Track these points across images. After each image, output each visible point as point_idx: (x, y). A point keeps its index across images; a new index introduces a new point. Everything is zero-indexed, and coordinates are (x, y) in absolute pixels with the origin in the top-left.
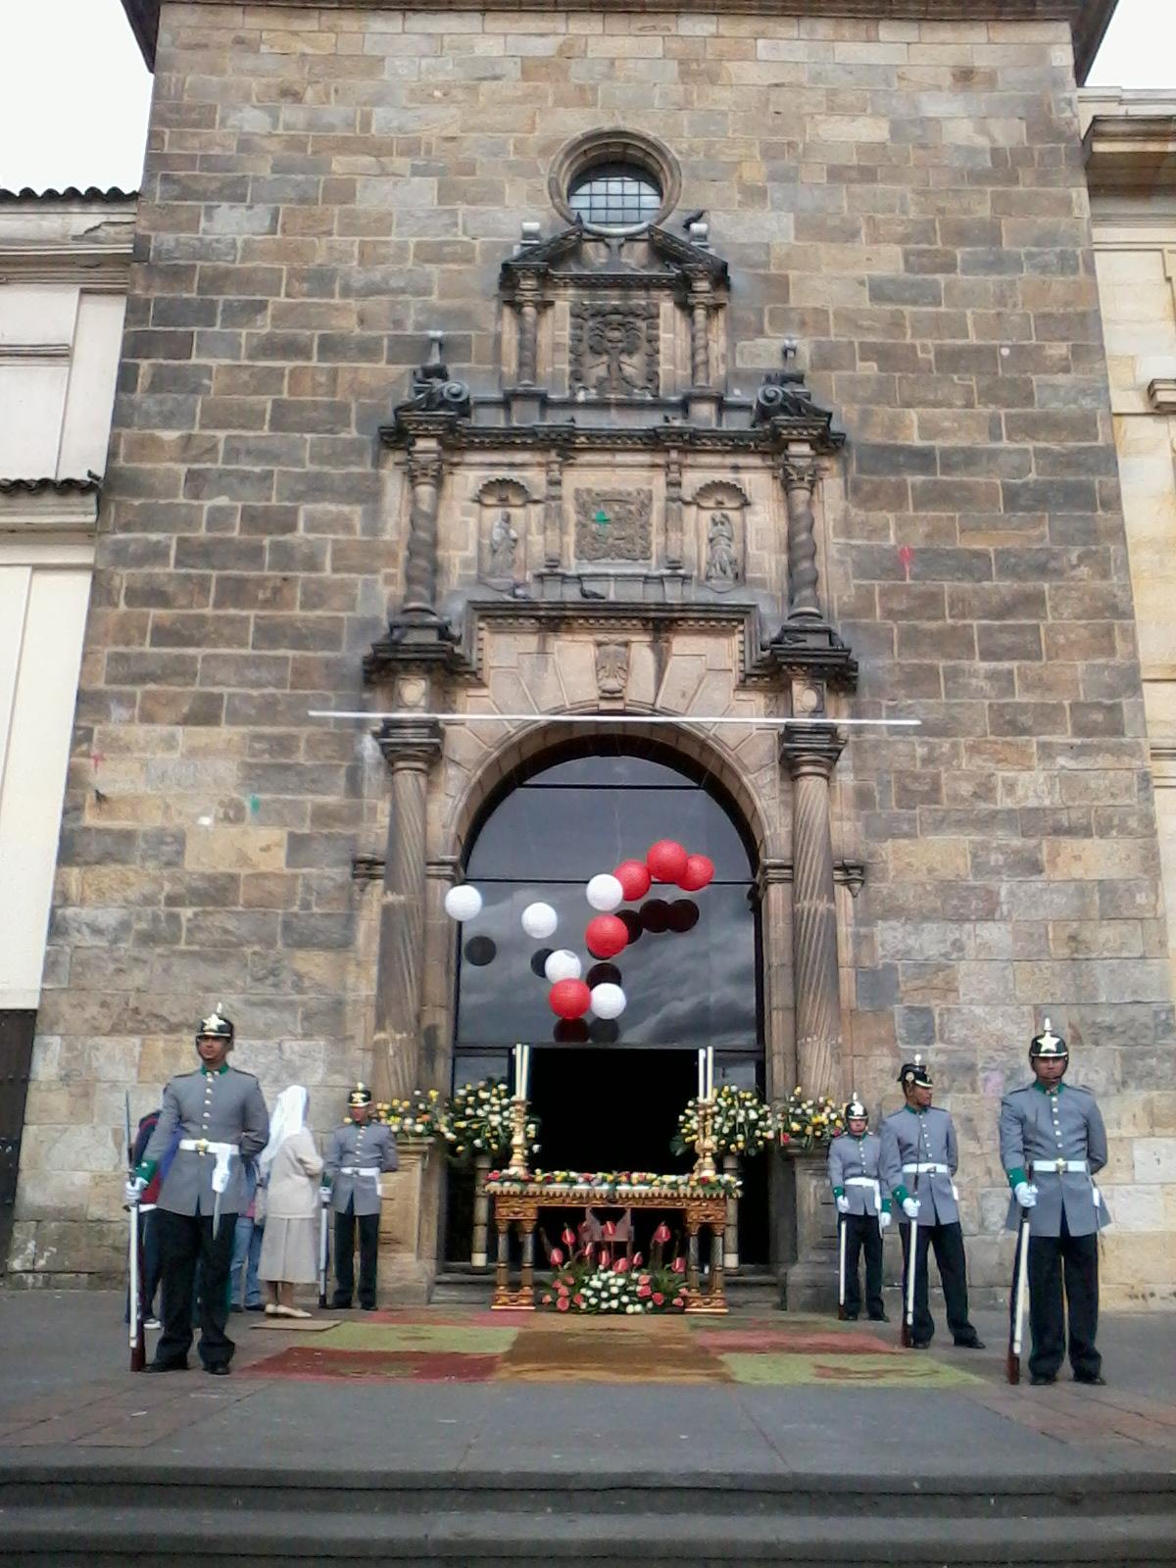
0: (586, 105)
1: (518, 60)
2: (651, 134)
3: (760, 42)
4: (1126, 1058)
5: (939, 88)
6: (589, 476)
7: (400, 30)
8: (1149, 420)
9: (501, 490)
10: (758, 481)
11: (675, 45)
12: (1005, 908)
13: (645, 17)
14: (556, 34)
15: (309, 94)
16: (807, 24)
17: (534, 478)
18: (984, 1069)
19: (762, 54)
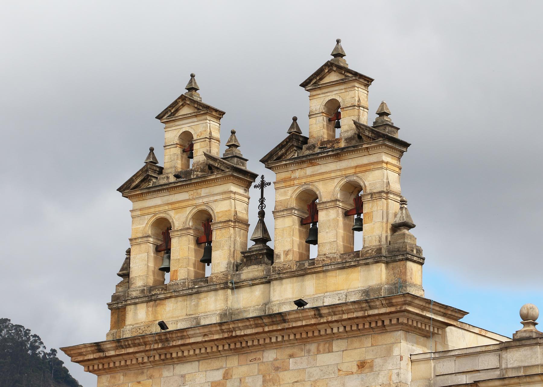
1: (210, 383)
3: (291, 359)
7: (172, 374)
11: (262, 367)
13: (252, 354)
16: (308, 347)
19: (292, 366)
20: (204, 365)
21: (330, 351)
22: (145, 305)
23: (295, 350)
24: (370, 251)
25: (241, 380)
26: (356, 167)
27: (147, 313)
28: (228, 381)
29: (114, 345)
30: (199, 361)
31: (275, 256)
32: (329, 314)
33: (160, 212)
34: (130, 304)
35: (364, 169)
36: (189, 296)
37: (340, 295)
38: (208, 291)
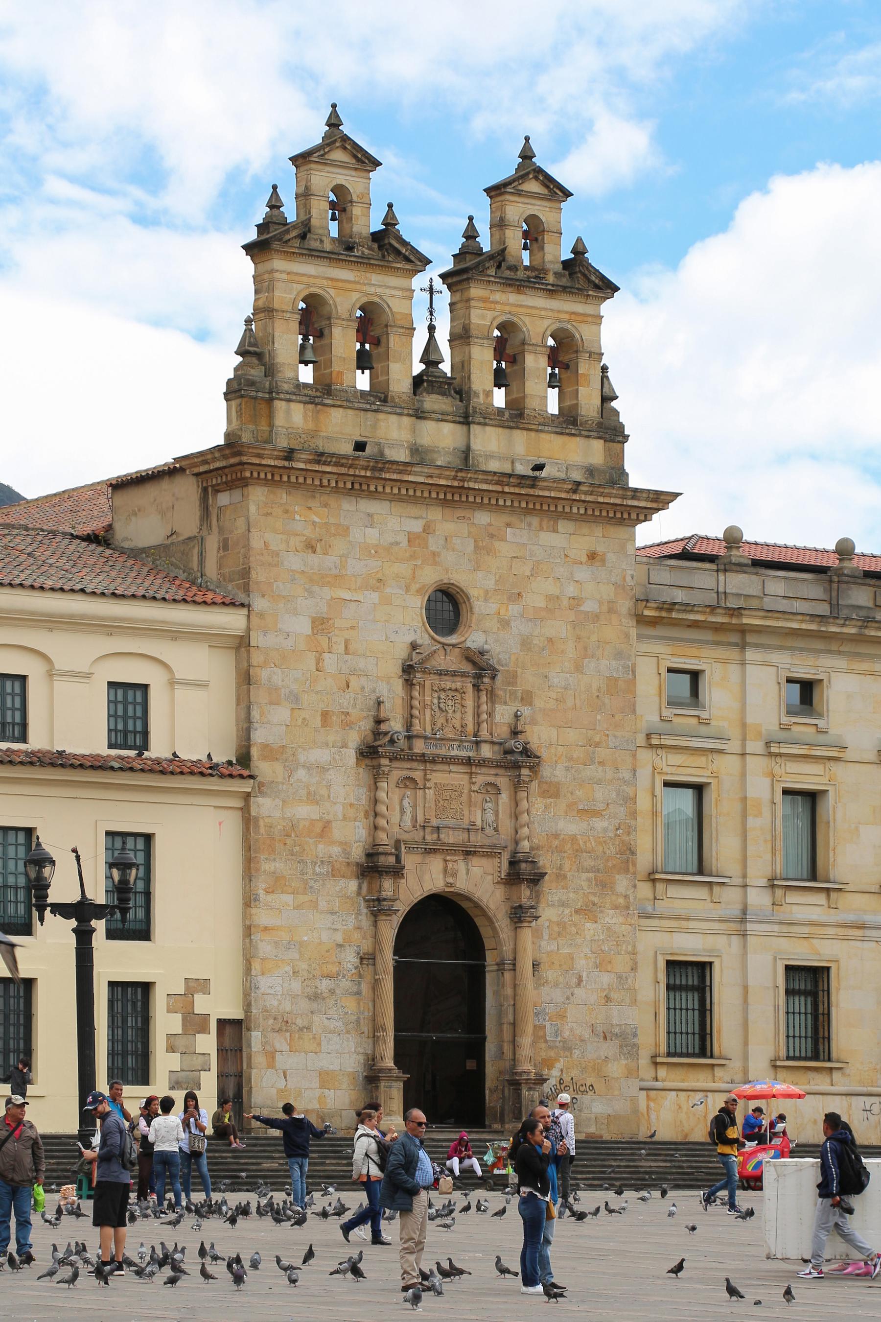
0: (435, 563)
2: (462, 585)
4: (621, 1046)
5: (581, 563)
6: (440, 776)
8: (645, 750)
9: (408, 782)
10: (503, 782)
12: (584, 982)
14: (422, 518)
15: (318, 549)
16: (529, 519)
17: (418, 775)
18: (575, 1049)
19: (509, 537)
20: (397, 508)
21: (555, 531)
22: (302, 405)
23: (514, 519)
24: (590, 422)
25: (446, 539)
26: (572, 313)
27: (305, 416)
28: (430, 536)
29: (311, 457)
30: (391, 501)
31: (472, 393)
32: (586, 493)
33: (314, 285)
34: (281, 399)
35: (580, 318)
36: (362, 412)
37: (560, 466)
38: (390, 413)
